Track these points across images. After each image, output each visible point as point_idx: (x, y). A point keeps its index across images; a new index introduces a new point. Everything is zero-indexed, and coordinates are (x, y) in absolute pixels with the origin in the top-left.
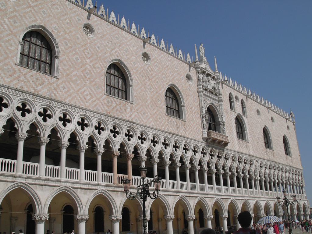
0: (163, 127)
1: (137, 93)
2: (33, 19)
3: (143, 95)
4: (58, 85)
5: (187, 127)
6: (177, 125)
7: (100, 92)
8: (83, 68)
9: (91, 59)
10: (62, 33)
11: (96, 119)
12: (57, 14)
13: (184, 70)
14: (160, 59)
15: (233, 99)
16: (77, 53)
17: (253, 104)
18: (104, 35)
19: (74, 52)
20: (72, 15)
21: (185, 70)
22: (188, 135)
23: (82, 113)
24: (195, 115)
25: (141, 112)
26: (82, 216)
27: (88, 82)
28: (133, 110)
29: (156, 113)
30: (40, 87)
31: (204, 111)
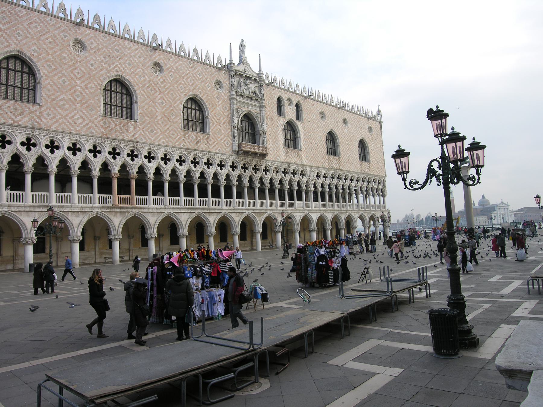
0: (177, 144)
2: (6, 44)
3: (152, 110)
4: (41, 113)
5: (210, 140)
6: (196, 139)
7: (94, 114)
8: (72, 91)
9: (82, 79)
10: (44, 55)
11: (90, 142)
12: (35, 34)
13: (211, 75)
14: (177, 68)
15: (284, 102)
16: (64, 75)
17: (315, 106)
18: (99, 50)
19: (60, 75)
20: (56, 32)
21: (213, 76)
22: (213, 149)
23: (72, 138)
25: (148, 129)
26: (74, 237)
27: (78, 105)
28: (138, 129)
29: (168, 129)
30: (20, 117)
31: (236, 121)
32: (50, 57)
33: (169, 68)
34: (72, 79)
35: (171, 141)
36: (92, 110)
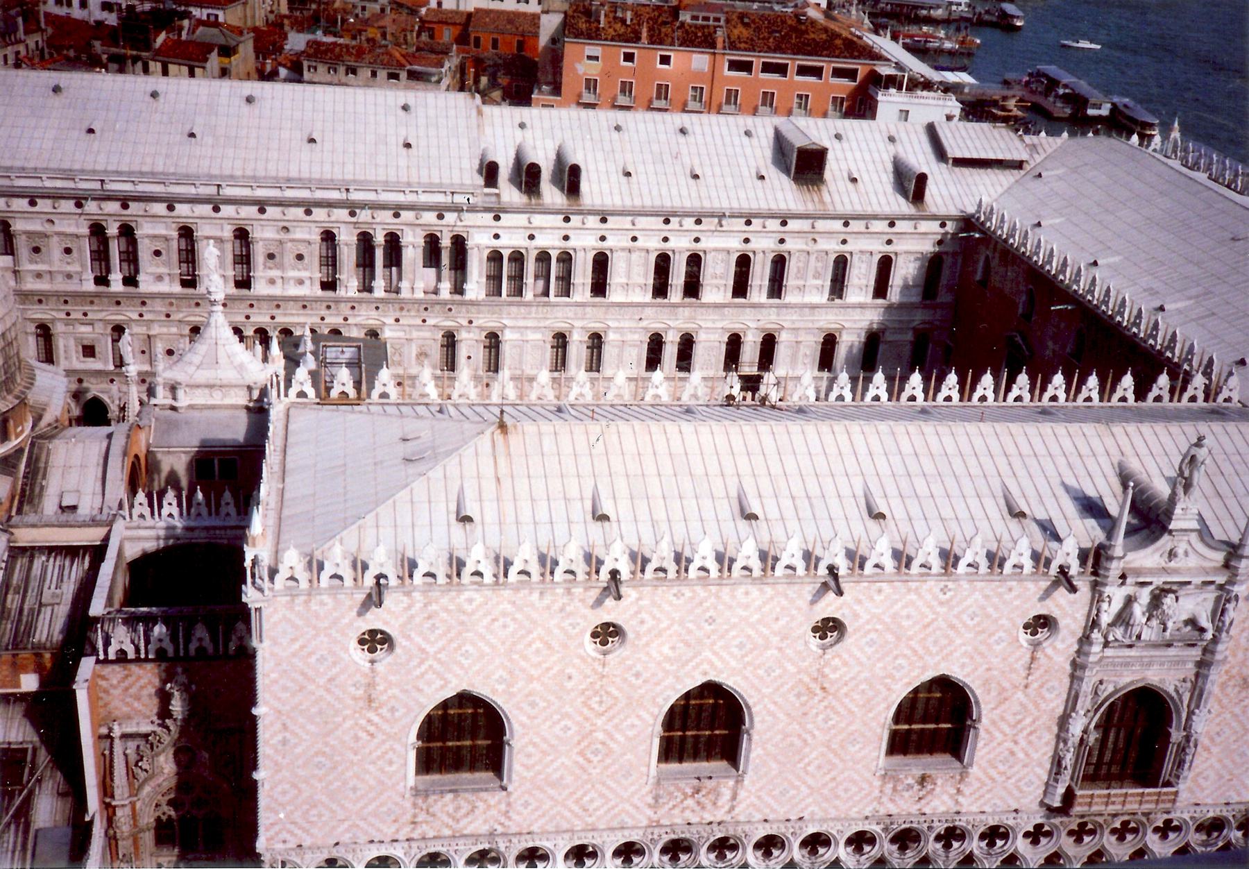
0: (855, 810)
1: (764, 749)
2: (439, 683)
3: (792, 745)
4: (509, 804)
5: (970, 784)
7: (632, 784)
8: (583, 744)
9: (611, 713)
10: (520, 684)
12: (503, 643)
14: (895, 616)
16: (567, 716)
20: (553, 622)
24: (1030, 743)
29: (834, 779)
32: (536, 685)
33: (868, 622)
34: (587, 719)
35: (835, 807)
36: (627, 775)
